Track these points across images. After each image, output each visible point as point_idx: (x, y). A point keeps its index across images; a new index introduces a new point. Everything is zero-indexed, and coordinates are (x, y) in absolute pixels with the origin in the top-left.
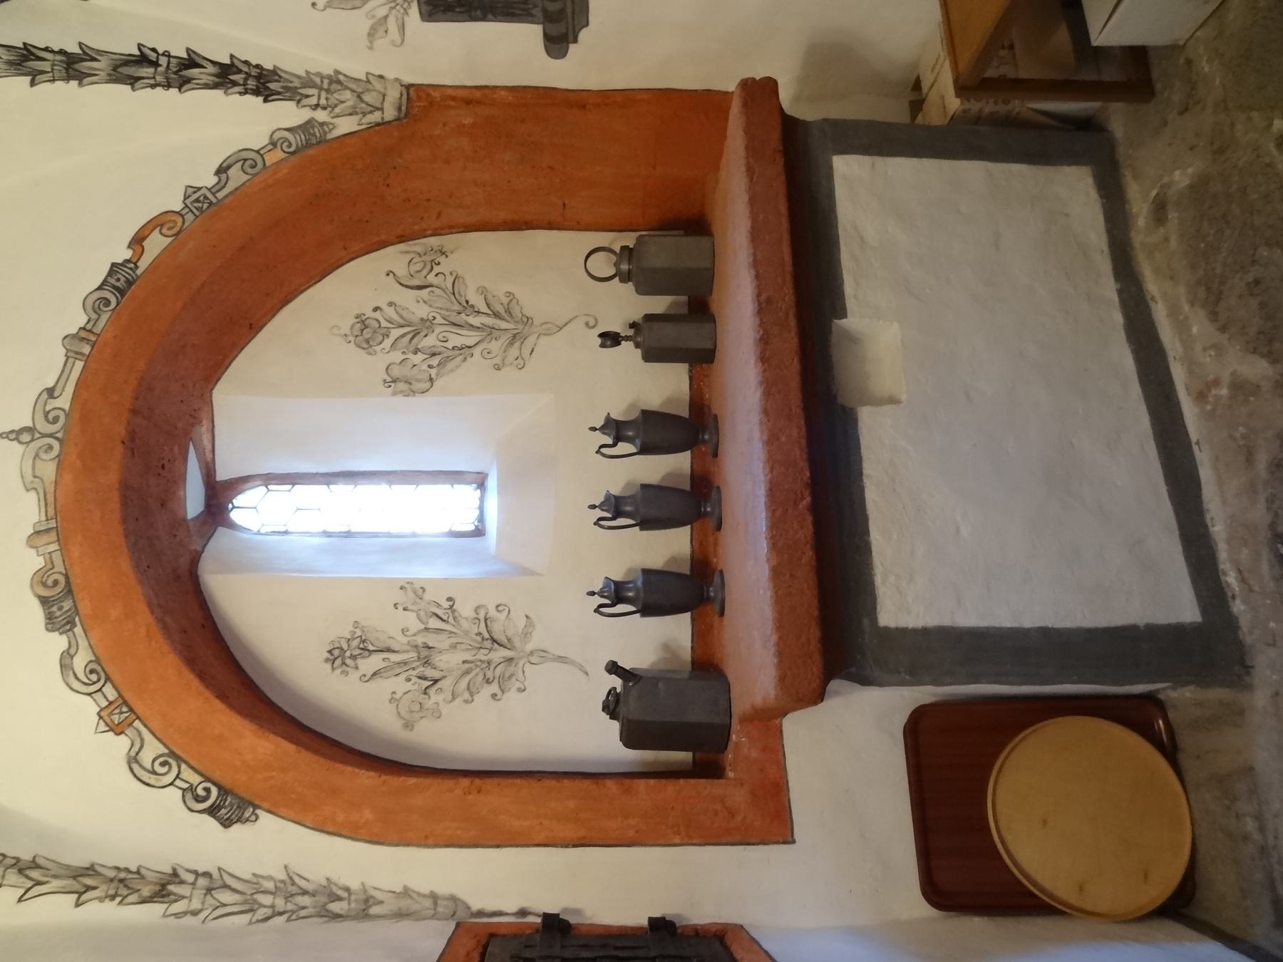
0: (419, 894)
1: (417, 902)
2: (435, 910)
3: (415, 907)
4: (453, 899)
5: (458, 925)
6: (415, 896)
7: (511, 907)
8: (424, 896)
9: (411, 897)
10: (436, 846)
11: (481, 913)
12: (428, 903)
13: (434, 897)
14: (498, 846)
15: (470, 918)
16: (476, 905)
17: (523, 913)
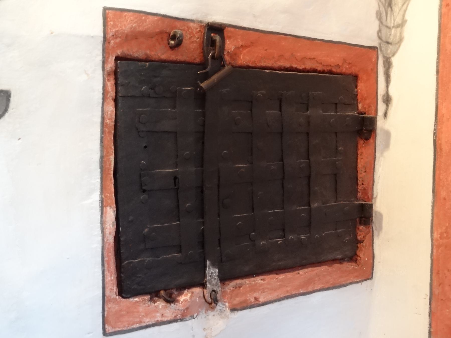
0: (405, 11)
1: (400, 10)
2: (393, 27)
3: (396, 9)
4: (401, 40)
5: (373, 48)
6: (404, 8)
7: (392, 92)
8: (404, 16)
9: (403, 5)
10: (441, 16)
11: (388, 65)
12: (398, 20)
13: (402, 25)
14: (438, 72)
15: (384, 57)
16: (395, 60)
17: (387, 100)
